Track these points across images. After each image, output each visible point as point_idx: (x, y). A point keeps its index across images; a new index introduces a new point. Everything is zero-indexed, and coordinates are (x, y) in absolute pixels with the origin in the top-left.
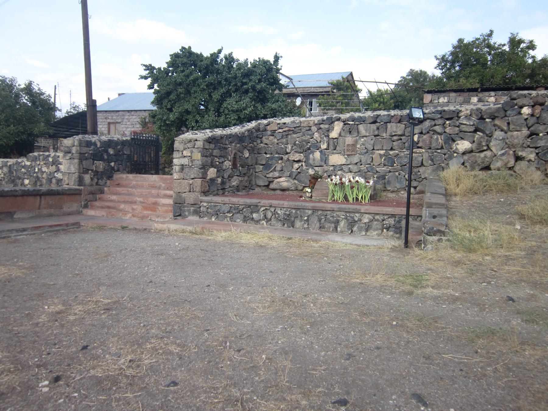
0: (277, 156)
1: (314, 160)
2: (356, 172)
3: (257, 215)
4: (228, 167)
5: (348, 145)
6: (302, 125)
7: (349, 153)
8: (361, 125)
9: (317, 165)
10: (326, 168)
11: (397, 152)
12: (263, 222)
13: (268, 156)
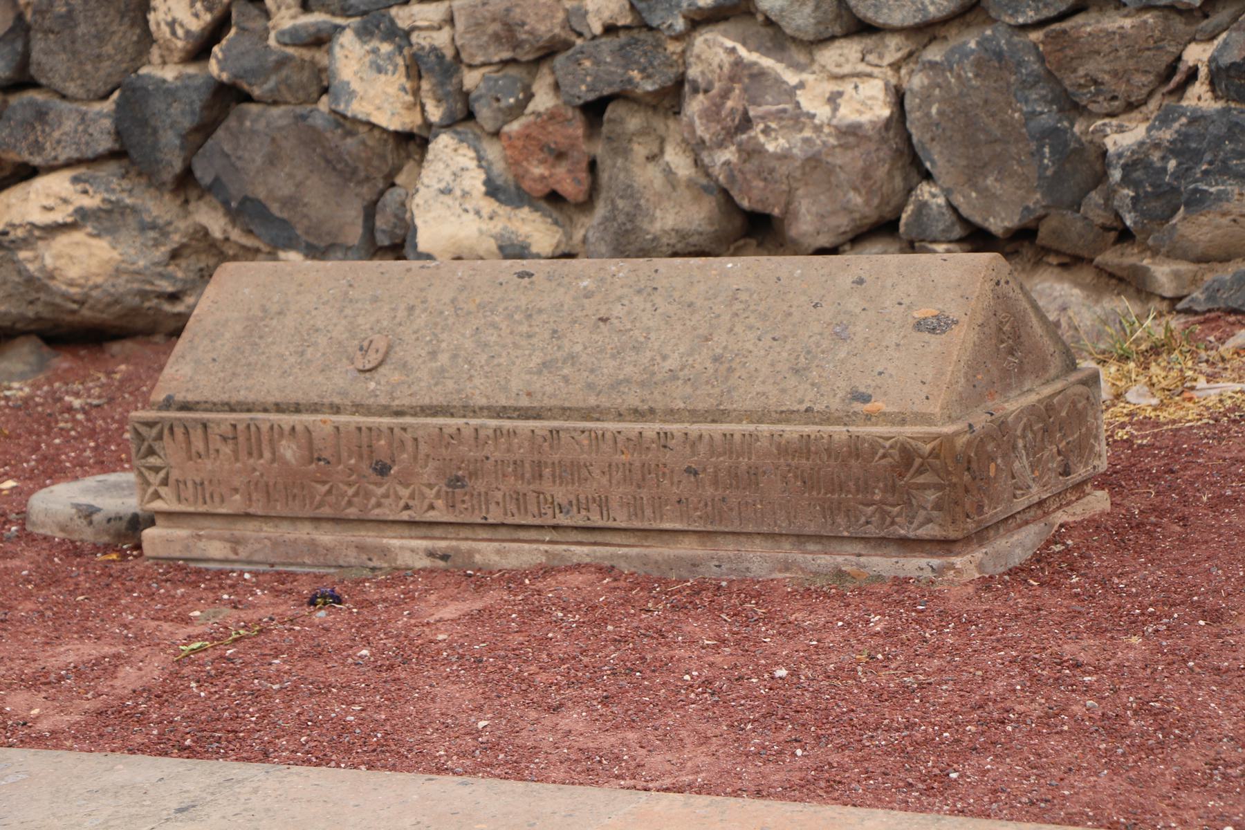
2: (926, 30)
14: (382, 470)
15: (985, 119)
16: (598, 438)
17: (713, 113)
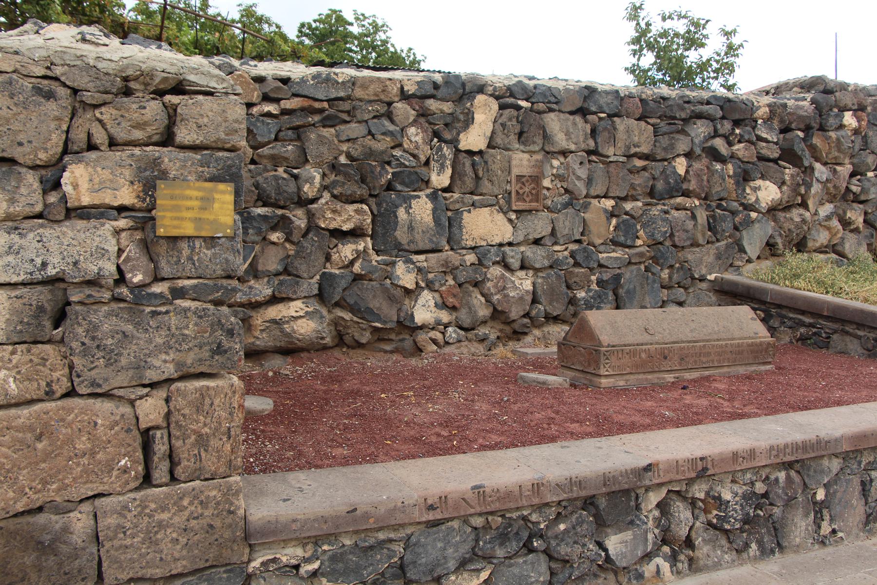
0: (261, 211)
1: (411, 228)
5: (519, 177)
6: (359, 93)
7: (520, 206)
8: (552, 115)
9: (421, 246)
10: (454, 258)
11: (640, 204)
12: (659, 560)
14: (665, 358)
16: (713, 346)
17: (496, 286)
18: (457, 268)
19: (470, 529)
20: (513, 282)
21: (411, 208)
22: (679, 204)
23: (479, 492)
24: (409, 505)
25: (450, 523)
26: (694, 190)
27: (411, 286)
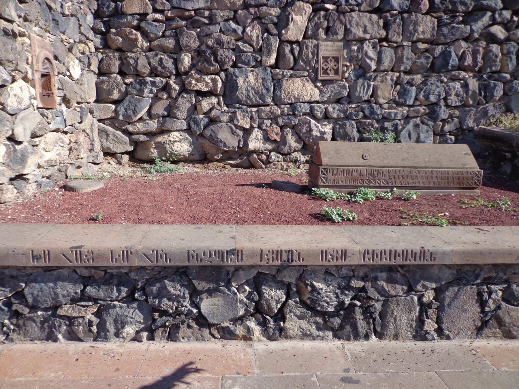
0: (152, 79)
3: (217, 300)
4: (26, 102)
5: (325, 58)
8: (353, 14)
13: (129, 80)
15: (349, 132)
18: (279, 116)
19: (78, 276)
20: (317, 127)
21: (247, 77)
22: (454, 75)
23: (76, 252)
24: (18, 254)
25: (60, 270)
26: (469, 65)
27: (248, 126)
